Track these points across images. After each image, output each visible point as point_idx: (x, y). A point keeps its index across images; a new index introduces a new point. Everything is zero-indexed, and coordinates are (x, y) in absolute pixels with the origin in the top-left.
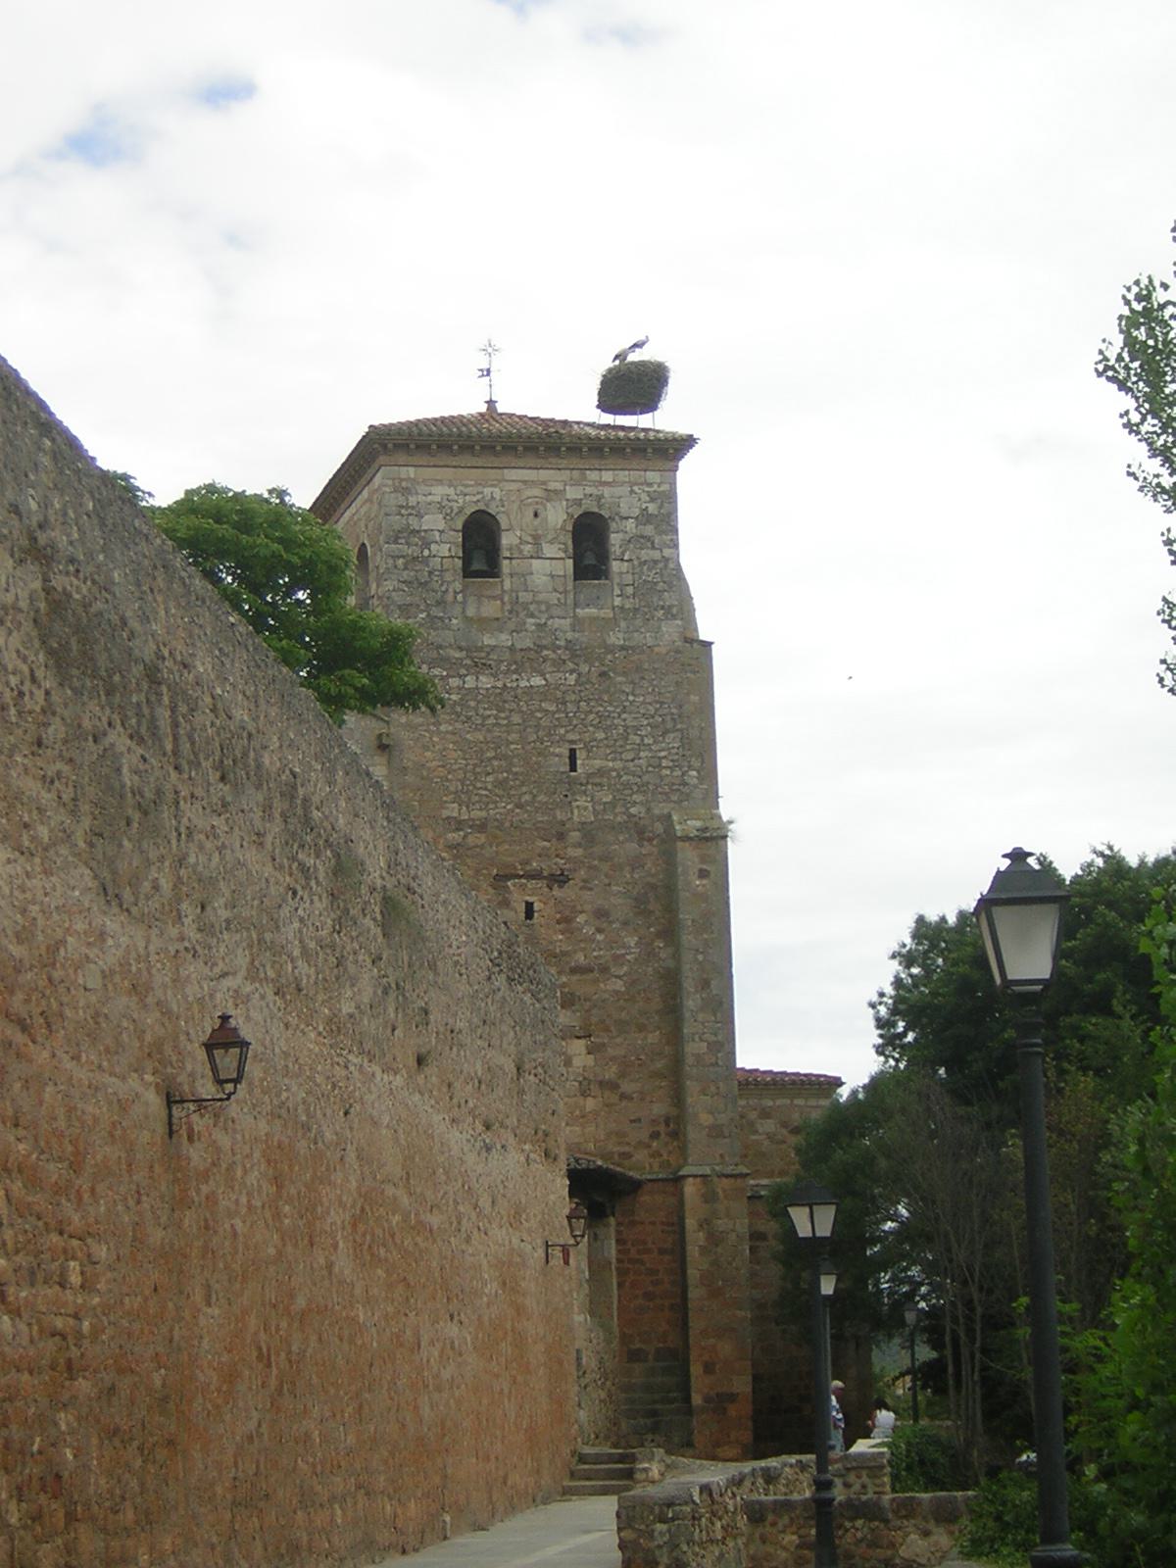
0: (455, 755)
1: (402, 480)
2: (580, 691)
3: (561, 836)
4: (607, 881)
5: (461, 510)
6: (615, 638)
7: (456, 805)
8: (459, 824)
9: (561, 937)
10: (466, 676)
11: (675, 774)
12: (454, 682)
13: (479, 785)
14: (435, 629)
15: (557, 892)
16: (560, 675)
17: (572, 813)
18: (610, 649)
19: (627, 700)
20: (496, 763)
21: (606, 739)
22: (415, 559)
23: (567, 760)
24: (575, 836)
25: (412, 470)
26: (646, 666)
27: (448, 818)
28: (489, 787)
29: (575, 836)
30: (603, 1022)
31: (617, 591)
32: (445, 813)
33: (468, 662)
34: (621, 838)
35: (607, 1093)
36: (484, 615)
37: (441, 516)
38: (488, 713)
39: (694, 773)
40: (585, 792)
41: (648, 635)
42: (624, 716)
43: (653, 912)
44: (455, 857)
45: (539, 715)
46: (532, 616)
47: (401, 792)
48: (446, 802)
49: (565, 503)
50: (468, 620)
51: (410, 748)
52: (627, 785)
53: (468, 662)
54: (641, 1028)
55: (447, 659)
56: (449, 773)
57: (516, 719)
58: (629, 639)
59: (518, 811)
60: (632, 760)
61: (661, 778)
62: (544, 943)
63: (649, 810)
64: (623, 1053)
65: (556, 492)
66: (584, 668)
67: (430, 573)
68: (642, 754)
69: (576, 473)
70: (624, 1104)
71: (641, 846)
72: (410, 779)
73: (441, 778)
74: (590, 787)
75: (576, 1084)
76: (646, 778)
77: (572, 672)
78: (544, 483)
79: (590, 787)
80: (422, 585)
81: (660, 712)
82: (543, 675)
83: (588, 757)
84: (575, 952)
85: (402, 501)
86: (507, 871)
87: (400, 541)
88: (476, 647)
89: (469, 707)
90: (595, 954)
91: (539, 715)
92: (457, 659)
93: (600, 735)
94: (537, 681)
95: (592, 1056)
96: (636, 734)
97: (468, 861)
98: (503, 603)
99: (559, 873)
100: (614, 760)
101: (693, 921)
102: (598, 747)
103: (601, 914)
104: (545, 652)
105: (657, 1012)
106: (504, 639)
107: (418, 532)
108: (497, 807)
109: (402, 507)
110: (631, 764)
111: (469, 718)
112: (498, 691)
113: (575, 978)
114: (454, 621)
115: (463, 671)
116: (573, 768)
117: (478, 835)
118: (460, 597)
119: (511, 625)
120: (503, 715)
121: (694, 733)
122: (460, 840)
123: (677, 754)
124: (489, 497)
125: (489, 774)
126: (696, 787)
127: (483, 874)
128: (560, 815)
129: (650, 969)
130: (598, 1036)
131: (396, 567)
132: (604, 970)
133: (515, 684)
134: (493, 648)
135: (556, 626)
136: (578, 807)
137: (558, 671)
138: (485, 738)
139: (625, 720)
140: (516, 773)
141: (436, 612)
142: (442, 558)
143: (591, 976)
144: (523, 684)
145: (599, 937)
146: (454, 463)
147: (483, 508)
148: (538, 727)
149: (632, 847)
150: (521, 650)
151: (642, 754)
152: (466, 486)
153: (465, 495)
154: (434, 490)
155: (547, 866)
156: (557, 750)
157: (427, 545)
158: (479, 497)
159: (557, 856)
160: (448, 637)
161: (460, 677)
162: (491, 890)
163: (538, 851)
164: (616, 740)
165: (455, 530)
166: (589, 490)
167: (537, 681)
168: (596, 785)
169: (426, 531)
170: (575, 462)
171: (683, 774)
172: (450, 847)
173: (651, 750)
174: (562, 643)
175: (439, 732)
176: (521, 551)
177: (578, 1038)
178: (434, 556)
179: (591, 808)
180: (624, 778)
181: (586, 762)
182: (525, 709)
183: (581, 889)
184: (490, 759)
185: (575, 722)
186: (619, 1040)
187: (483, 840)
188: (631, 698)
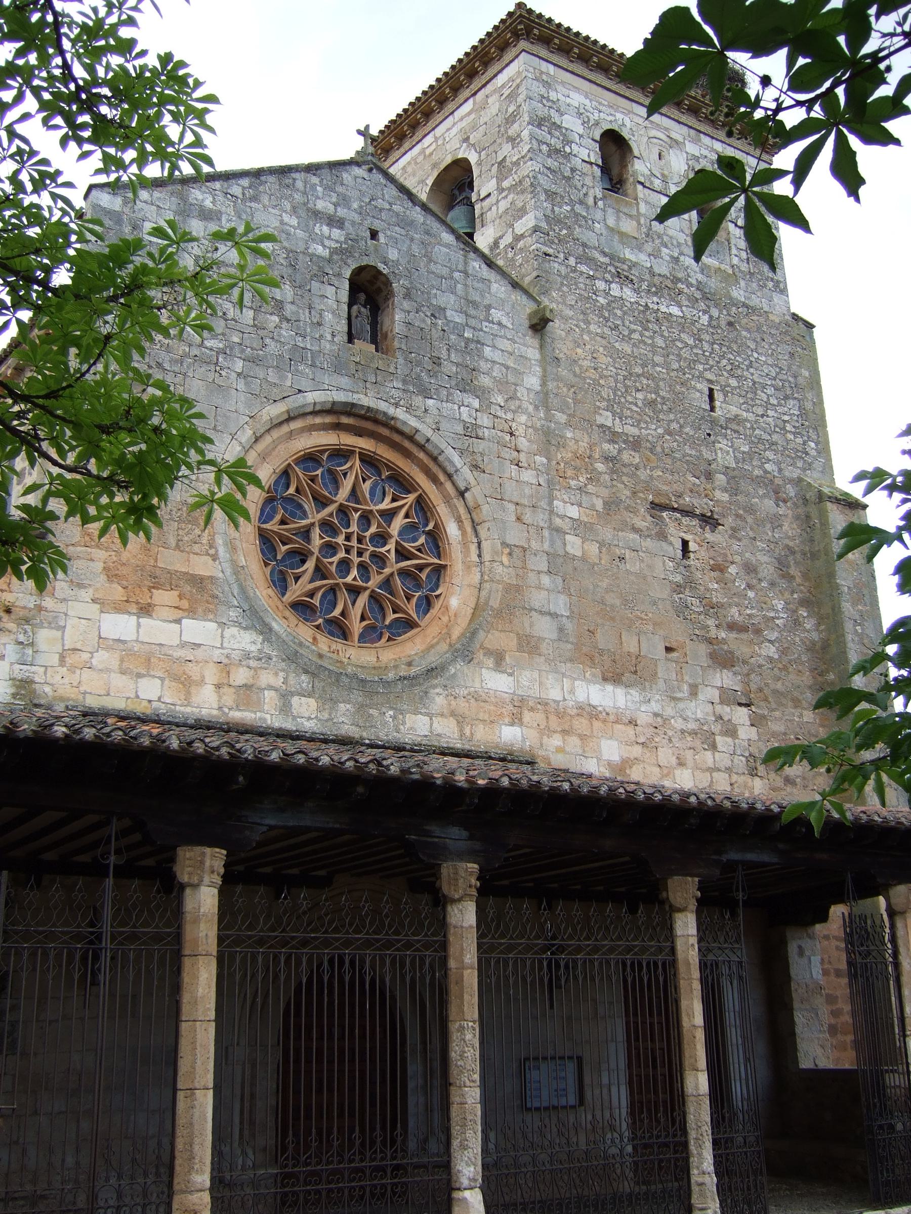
0: (604, 360)
1: (542, 73)
2: (712, 333)
3: (709, 476)
4: (751, 534)
5: (597, 123)
6: (738, 294)
7: (609, 414)
8: (614, 437)
9: (716, 586)
10: (611, 282)
11: (797, 440)
12: (601, 285)
13: (629, 398)
14: (580, 226)
15: (709, 536)
16: (695, 312)
17: (716, 454)
18: (735, 303)
19: (752, 355)
20: (645, 381)
21: (739, 387)
22: (557, 151)
23: (707, 399)
24: (720, 479)
25: (551, 67)
26: (765, 328)
27: (601, 426)
28: (640, 404)
29: (720, 479)
30: (761, 690)
31: (734, 251)
32: (600, 420)
33: (613, 270)
34: (761, 493)
35: (772, 775)
36: (623, 229)
37: (580, 122)
38: (633, 327)
39: (812, 445)
40: (725, 436)
41: (763, 300)
42: (752, 370)
43: (793, 577)
44: (613, 471)
45: (680, 345)
46: (666, 247)
47: (555, 384)
48: (599, 408)
49: (685, 155)
50: (611, 230)
51: (561, 339)
52: (760, 440)
53: (613, 270)
54: (797, 703)
55: (593, 259)
56: (601, 377)
57: (660, 342)
58: (749, 298)
59: (668, 437)
60: (762, 416)
61: (788, 441)
62: (702, 588)
63: (780, 470)
64: (782, 729)
65: (676, 142)
66: (715, 312)
67: (573, 170)
68: (770, 413)
69: (692, 132)
70: (788, 790)
71: (778, 506)
72: (563, 372)
73: (594, 380)
74: (729, 432)
75: (743, 759)
76: (775, 437)
77: (705, 312)
78: (667, 129)
79: (729, 432)
80: (568, 179)
81: (780, 376)
82: (680, 306)
83: (725, 402)
84: (730, 605)
85: (543, 91)
86: (662, 500)
87: (543, 128)
88: (619, 257)
89: (615, 314)
90: (748, 612)
91: (680, 345)
92: (602, 263)
93: (733, 382)
94: (675, 310)
95: (754, 729)
96: (763, 392)
97: (625, 478)
98: (639, 224)
99: (709, 514)
100: (747, 411)
101: (849, 588)
102: (733, 394)
103: (750, 569)
104: (680, 285)
105: (810, 687)
106: (643, 259)
107: (560, 127)
108: (647, 428)
109: (543, 97)
110: (762, 420)
111: (617, 327)
112: (641, 308)
113: (733, 635)
114: (596, 225)
115: (608, 277)
116: (712, 409)
117: (633, 453)
118: (600, 203)
119: (649, 247)
120: (647, 334)
121: (809, 406)
122: (615, 453)
123: (797, 421)
124: (620, 122)
125: (638, 390)
126: (815, 458)
127: (640, 498)
128: (707, 454)
129: (797, 639)
130: (758, 707)
131: (540, 150)
132: (758, 632)
133: (656, 307)
134: (635, 265)
135: (687, 264)
136: (721, 449)
137: (693, 308)
138: (633, 352)
139: (752, 374)
140: (663, 398)
141: (578, 208)
142: (583, 161)
143: (744, 636)
144: (663, 309)
145: (751, 594)
146: (589, 77)
147: (617, 129)
148: (679, 355)
149: (769, 504)
150: (660, 275)
151: (770, 413)
152: (600, 104)
153: (600, 112)
154: (572, 94)
155: (701, 505)
156: (699, 386)
157: (569, 142)
158: (612, 118)
159: (706, 496)
160: (591, 238)
161: (606, 281)
162: (649, 518)
163: (689, 485)
164: (747, 392)
165: (593, 140)
166: (705, 152)
167: (675, 310)
168: (735, 431)
169: (567, 129)
170: (691, 121)
171: (805, 443)
172: (607, 459)
173: (776, 411)
174: (694, 282)
175: (589, 332)
176: (652, 183)
177: (740, 704)
178: (575, 156)
179: (731, 452)
180: (757, 432)
181: (724, 405)
182: (666, 334)
183: (731, 537)
184: (638, 376)
185: (711, 362)
186: (777, 714)
187: (637, 460)
188: (756, 355)
